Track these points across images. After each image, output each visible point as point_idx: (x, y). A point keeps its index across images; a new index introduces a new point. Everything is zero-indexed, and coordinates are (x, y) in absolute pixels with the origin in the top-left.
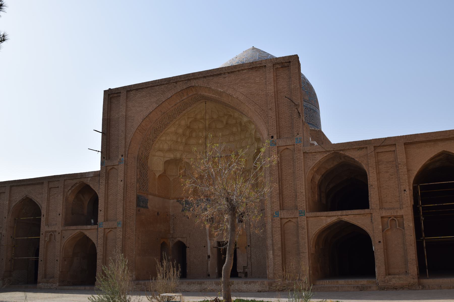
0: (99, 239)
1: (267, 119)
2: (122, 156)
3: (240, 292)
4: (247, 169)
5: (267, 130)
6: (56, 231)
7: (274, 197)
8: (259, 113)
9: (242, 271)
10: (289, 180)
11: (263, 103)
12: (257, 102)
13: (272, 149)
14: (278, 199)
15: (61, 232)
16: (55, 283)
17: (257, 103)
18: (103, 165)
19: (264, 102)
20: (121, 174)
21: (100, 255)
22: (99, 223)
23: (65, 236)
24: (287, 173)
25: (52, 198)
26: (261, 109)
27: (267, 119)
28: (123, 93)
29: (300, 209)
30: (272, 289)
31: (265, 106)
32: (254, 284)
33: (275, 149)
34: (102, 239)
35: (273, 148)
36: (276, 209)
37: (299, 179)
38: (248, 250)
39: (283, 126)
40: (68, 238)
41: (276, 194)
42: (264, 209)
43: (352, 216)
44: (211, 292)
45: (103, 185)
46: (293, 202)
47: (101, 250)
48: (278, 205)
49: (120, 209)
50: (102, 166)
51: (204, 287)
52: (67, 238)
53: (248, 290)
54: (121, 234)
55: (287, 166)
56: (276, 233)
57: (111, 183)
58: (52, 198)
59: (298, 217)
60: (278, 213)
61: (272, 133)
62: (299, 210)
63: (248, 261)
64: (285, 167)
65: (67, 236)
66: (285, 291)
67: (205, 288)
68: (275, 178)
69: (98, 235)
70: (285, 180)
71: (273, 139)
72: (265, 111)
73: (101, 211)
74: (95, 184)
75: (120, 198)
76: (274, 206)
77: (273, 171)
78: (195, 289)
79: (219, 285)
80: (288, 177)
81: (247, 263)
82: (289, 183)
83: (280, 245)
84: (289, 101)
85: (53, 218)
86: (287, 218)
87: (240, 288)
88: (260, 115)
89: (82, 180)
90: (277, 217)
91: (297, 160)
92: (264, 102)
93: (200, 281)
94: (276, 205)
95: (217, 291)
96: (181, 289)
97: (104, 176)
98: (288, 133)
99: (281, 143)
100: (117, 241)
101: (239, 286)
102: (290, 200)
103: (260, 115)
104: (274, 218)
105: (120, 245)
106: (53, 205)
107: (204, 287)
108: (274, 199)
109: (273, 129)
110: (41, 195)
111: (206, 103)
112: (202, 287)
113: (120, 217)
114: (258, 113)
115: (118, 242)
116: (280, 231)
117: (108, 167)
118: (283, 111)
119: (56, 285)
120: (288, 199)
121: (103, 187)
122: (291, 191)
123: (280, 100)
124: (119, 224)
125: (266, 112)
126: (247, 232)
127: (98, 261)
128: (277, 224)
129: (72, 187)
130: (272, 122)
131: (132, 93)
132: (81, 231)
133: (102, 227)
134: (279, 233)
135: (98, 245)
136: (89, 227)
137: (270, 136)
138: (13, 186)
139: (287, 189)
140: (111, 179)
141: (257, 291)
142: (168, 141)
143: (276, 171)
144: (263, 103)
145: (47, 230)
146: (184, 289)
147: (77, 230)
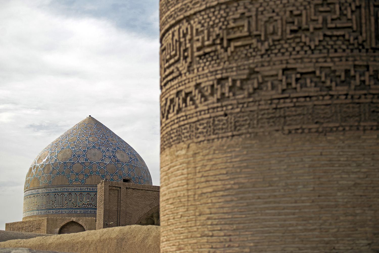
28: (123, 189)
131: (129, 190)
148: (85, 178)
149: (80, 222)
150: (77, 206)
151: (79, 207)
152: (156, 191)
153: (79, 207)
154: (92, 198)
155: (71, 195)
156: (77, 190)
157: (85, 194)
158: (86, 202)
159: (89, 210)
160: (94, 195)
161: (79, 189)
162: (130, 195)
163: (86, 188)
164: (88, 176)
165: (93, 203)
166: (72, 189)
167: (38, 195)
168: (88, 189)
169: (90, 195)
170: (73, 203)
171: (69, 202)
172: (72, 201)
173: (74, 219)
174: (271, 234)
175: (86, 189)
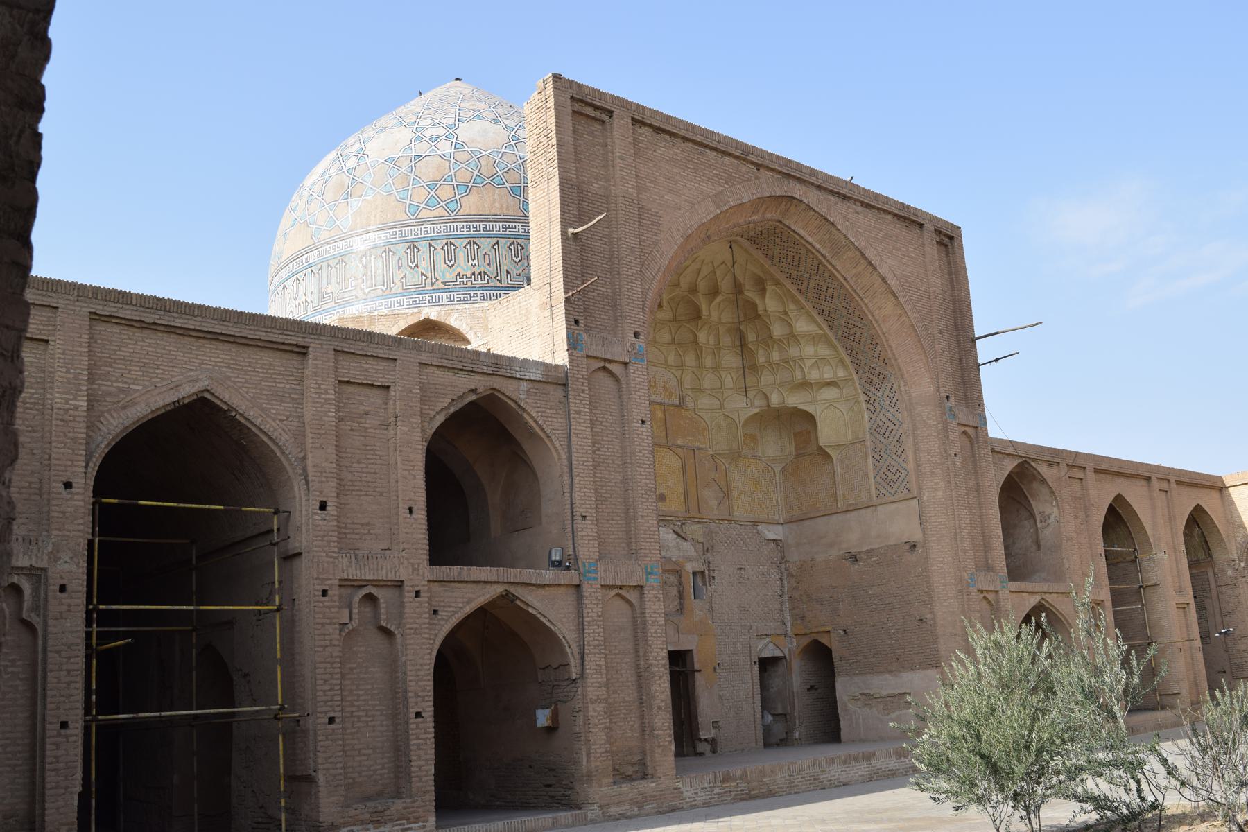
0: (589, 626)
6: (399, 585)
15: (429, 591)
16: (417, 820)
18: (575, 349)
21: (597, 685)
23: (444, 606)
25: (352, 430)
28: (622, 119)
34: (599, 626)
43: (1055, 595)
45: (584, 422)
47: (600, 666)
50: (575, 353)
52: (450, 617)
57: (597, 420)
58: (352, 430)
65: (451, 609)
73: (584, 517)
74: (548, 411)
75: (644, 481)
78: (860, 773)
79: (900, 758)
85: (362, 524)
89: (497, 383)
96: (831, 780)
97: (583, 391)
105: (662, 649)
106: (359, 462)
110: (282, 401)
111: (731, 247)
113: (650, 549)
115: (652, 636)
119: (424, 827)
121: (581, 430)
124: (650, 573)
127: (594, 710)
132: (512, 589)
133: (596, 579)
135: (586, 647)
137: (944, 395)
138: (108, 319)
145: (353, 573)
146: (838, 779)
147: (496, 586)
148: (457, 197)
149: (452, 320)
150: (439, 282)
151: (444, 283)
152: (730, 155)
153: (444, 283)
154: (487, 257)
155: (416, 250)
156: (436, 234)
157: (462, 243)
158: (465, 268)
159: (478, 292)
160: (493, 247)
161: (442, 230)
162: (647, 148)
163: (465, 224)
164: (468, 190)
165: (491, 269)
166: (419, 232)
167: (310, 270)
168: (472, 229)
169: (479, 247)
170: (422, 274)
171: (410, 272)
172: (420, 270)
173: (432, 314)
174: (839, 479)
175: (465, 229)
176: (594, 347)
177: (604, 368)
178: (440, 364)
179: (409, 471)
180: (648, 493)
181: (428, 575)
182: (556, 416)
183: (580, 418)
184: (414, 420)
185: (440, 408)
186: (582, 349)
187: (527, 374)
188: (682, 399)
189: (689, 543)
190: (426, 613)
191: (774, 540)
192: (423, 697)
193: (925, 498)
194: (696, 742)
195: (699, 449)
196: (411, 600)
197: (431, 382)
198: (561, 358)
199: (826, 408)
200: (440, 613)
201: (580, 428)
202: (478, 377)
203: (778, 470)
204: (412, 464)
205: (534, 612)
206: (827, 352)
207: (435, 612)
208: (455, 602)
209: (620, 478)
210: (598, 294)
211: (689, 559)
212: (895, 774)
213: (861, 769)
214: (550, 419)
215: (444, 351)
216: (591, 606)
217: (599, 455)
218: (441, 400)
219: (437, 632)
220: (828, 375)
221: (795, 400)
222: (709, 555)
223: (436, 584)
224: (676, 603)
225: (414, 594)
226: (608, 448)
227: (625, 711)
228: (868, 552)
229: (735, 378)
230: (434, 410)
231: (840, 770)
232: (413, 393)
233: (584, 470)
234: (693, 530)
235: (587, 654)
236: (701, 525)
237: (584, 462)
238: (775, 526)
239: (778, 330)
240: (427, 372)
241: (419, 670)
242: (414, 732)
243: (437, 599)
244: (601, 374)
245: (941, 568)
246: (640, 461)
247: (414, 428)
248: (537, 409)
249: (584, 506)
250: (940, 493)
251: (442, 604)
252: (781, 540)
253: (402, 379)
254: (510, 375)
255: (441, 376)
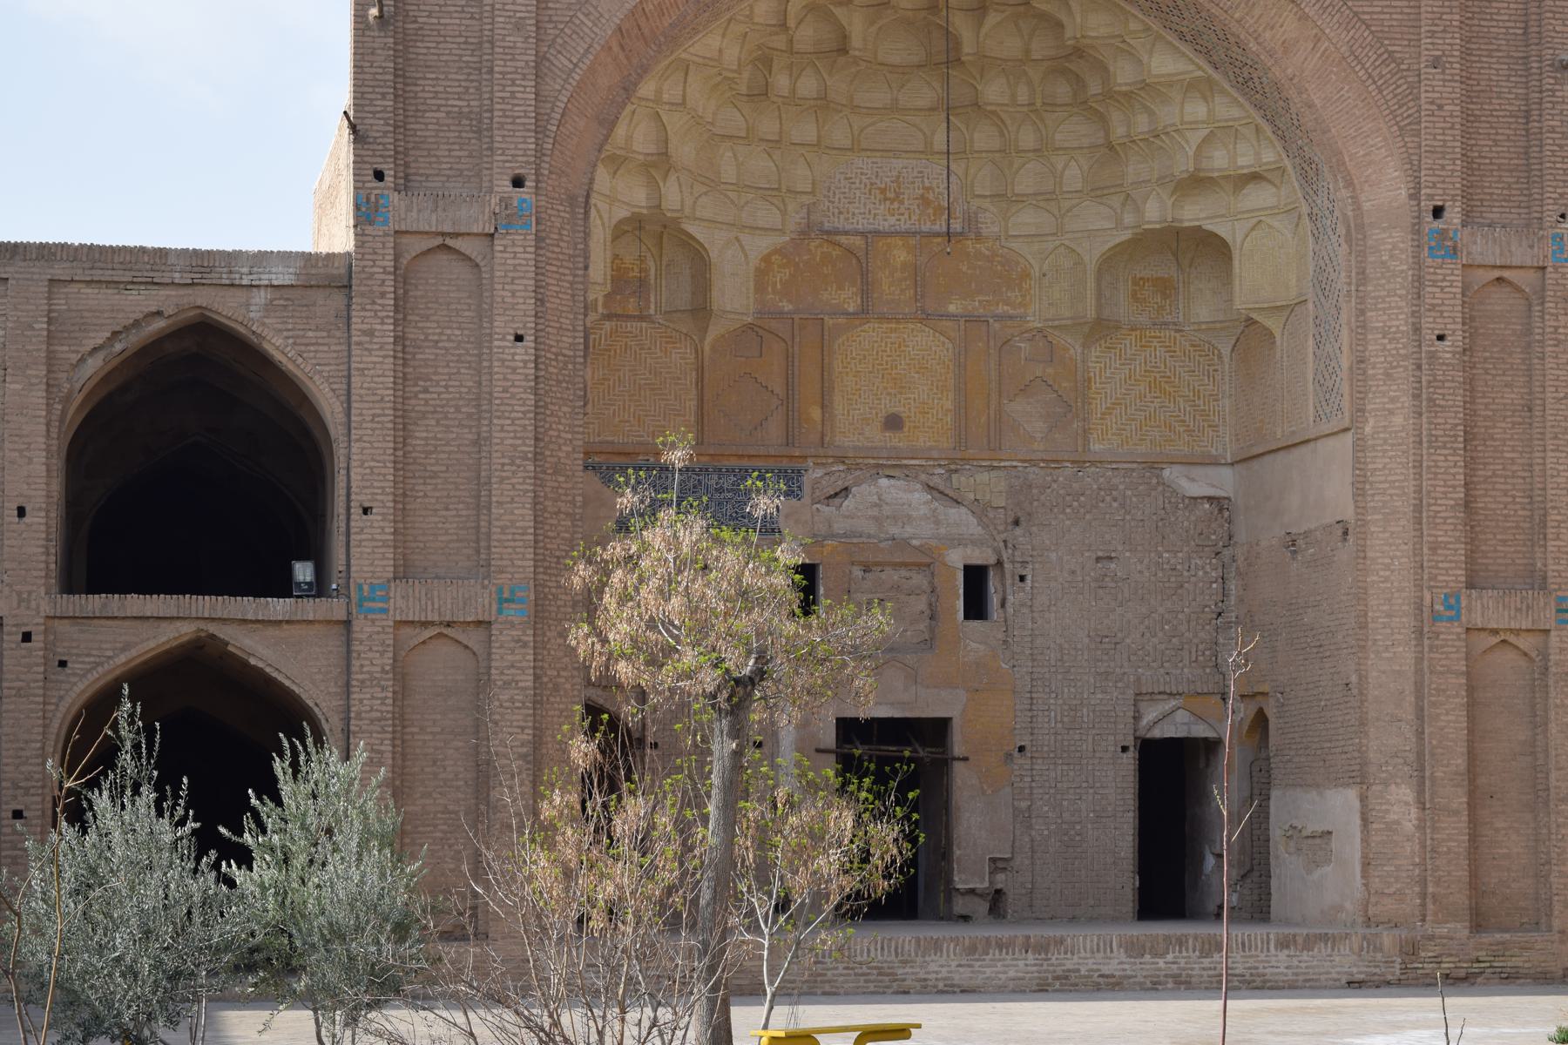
1: (1410, 112)
2: (518, 182)
3: (1257, 988)
4: (1031, 325)
5: (1410, 172)
7: (1438, 521)
8: (1375, 74)
9: (986, 884)
10: (1504, 440)
11: (1395, 23)
12: (1366, 9)
13: (1435, 274)
14: (1458, 534)
17: (1364, 13)
18: (371, 223)
19: (1400, 17)
20: (513, 296)
22: (360, 587)
24: (1493, 403)
26: (1383, 50)
27: (1409, 108)
29: (1560, 589)
30: (1420, 972)
31: (1402, 39)
32: (1326, 948)
33: (1452, 274)
34: (383, 689)
35: (1441, 268)
36: (1447, 582)
37: (1562, 442)
38: (1017, 773)
39: (1482, 161)
40: (100, 669)
41: (1452, 506)
42: (1111, 558)
44: (1098, 990)
46: (1519, 552)
48: (1461, 561)
49: (512, 513)
50: (369, 230)
51: (1060, 965)
52: (89, 671)
53: (1301, 978)
54: (524, 664)
55: (1495, 368)
56: (1442, 699)
57: (426, 340)
59: (1548, 631)
60: (1458, 602)
61: (1440, 192)
62: (1559, 593)
63: (1018, 833)
64: (1486, 372)
65: (92, 659)
66: (1479, 980)
67: (1069, 971)
68: (1448, 427)
69: (356, 663)
70: (1485, 440)
71: (1439, 224)
72: (1403, 67)
74: (310, 334)
75: (510, 442)
76: (1440, 565)
77: (1439, 391)
78: (1012, 974)
80: (1498, 425)
81: (1014, 842)
82: (1503, 458)
83: (1459, 761)
84: (1515, 34)
86: (1495, 632)
87: (1257, 968)
88: (1375, 82)
90: (1450, 620)
91: (1555, 346)
92: (1400, 17)
93: (1036, 933)
94: (1451, 561)
95: (1135, 983)
96: (925, 980)
97: (383, 295)
98: (1505, 200)
99: (1482, 248)
100: (497, 703)
101: (1251, 956)
102: (1500, 540)
103: (1375, 82)
104: (1439, 624)
105: (523, 728)
107: (1060, 965)
108: (1441, 533)
109: (1443, 168)
112: (1052, 965)
114: (1366, 70)
115: (501, 706)
116: (1464, 693)
117: (405, 240)
118: (1482, 83)
120: (1495, 534)
122: (1510, 499)
123: (1476, 22)
124: (507, 601)
125: (1408, 70)
126: (1017, 676)
128: (1452, 656)
129: (115, 334)
130: (1444, 134)
132: (212, 628)
133: (386, 611)
134: (1457, 700)
135: (352, 722)
136: (278, 607)
137: (1427, 206)
139: (1490, 487)
140: (427, 318)
141: (1344, 981)
142: (667, 107)
143: (1454, 388)
144: (1395, 23)
146: (945, 979)
147: (178, 624)
176: (414, 214)
177: (444, 247)
178: (88, 279)
179: (20, 451)
180: (518, 462)
181: (46, 608)
182: (326, 341)
183: (371, 343)
184: (34, 372)
185: (89, 349)
186: (385, 222)
187: (263, 277)
188: (971, 220)
189: (963, 510)
190: (37, 665)
191: (1210, 499)
192: (28, 789)
193: (1368, 430)
194: (954, 893)
195: (999, 318)
196: (14, 646)
197: (74, 307)
198: (338, 238)
199: (1253, 229)
200: (69, 665)
201: (369, 359)
202: (164, 292)
203: (1226, 351)
204: (27, 440)
205: (261, 665)
206: (1235, 112)
207: (63, 664)
208: (100, 649)
209: (470, 436)
210: (448, 113)
211: (960, 542)
212: (1118, 984)
213: (1023, 965)
214: (312, 348)
215: (97, 256)
216: (370, 655)
217: (426, 400)
218: (92, 335)
219: (62, 693)
220: (1246, 160)
221: (1194, 213)
222: (1018, 531)
223: (66, 621)
224: (922, 627)
225: (20, 637)
226: (446, 387)
227: (445, 827)
228: (1306, 534)
229: (1086, 168)
230: (78, 352)
231: (954, 964)
232: (33, 329)
233: (373, 430)
234: (989, 485)
235: (354, 733)
236: (1002, 473)
237: (374, 416)
238: (1210, 470)
239: (1124, 75)
240: (67, 293)
241: (22, 749)
242: (7, 838)
243: (66, 644)
244: (443, 258)
245: (1386, 580)
246: (502, 408)
247: (32, 385)
248: (285, 334)
249: (368, 491)
250: (1398, 420)
251: (75, 651)
252: (1228, 499)
253: (16, 309)
254: (227, 282)
255: (93, 297)
